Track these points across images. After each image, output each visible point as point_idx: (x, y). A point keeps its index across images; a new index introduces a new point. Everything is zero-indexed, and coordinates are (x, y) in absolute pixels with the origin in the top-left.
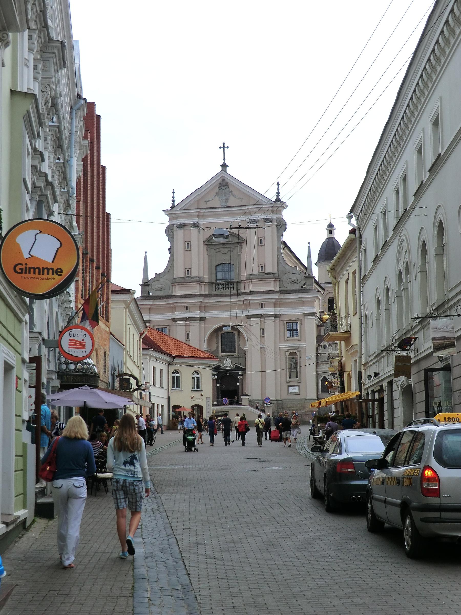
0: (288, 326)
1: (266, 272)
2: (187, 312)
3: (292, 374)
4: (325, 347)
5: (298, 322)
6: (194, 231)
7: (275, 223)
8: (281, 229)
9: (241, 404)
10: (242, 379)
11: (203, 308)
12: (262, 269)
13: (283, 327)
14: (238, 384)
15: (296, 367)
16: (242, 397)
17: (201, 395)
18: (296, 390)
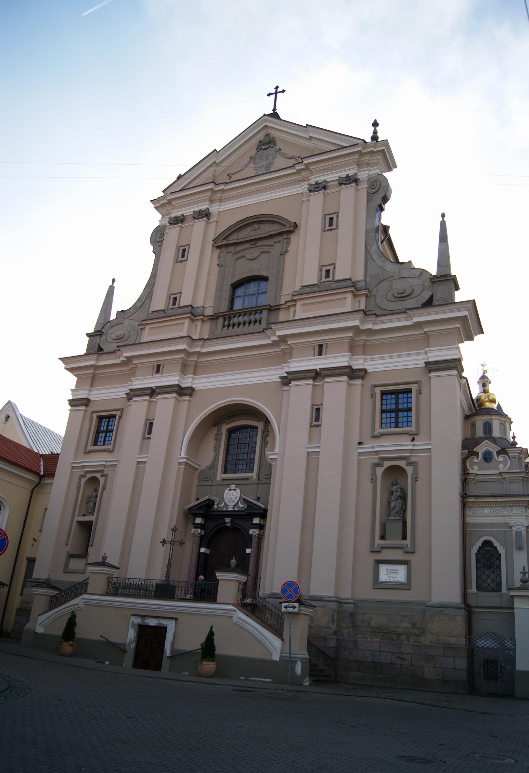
0: (384, 402)
1: (337, 278)
2: (158, 375)
4: (488, 457)
7: (364, 186)
8: (376, 196)
10: (260, 538)
11: (191, 369)
12: (327, 276)
14: (248, 551)
16: (219, 575)
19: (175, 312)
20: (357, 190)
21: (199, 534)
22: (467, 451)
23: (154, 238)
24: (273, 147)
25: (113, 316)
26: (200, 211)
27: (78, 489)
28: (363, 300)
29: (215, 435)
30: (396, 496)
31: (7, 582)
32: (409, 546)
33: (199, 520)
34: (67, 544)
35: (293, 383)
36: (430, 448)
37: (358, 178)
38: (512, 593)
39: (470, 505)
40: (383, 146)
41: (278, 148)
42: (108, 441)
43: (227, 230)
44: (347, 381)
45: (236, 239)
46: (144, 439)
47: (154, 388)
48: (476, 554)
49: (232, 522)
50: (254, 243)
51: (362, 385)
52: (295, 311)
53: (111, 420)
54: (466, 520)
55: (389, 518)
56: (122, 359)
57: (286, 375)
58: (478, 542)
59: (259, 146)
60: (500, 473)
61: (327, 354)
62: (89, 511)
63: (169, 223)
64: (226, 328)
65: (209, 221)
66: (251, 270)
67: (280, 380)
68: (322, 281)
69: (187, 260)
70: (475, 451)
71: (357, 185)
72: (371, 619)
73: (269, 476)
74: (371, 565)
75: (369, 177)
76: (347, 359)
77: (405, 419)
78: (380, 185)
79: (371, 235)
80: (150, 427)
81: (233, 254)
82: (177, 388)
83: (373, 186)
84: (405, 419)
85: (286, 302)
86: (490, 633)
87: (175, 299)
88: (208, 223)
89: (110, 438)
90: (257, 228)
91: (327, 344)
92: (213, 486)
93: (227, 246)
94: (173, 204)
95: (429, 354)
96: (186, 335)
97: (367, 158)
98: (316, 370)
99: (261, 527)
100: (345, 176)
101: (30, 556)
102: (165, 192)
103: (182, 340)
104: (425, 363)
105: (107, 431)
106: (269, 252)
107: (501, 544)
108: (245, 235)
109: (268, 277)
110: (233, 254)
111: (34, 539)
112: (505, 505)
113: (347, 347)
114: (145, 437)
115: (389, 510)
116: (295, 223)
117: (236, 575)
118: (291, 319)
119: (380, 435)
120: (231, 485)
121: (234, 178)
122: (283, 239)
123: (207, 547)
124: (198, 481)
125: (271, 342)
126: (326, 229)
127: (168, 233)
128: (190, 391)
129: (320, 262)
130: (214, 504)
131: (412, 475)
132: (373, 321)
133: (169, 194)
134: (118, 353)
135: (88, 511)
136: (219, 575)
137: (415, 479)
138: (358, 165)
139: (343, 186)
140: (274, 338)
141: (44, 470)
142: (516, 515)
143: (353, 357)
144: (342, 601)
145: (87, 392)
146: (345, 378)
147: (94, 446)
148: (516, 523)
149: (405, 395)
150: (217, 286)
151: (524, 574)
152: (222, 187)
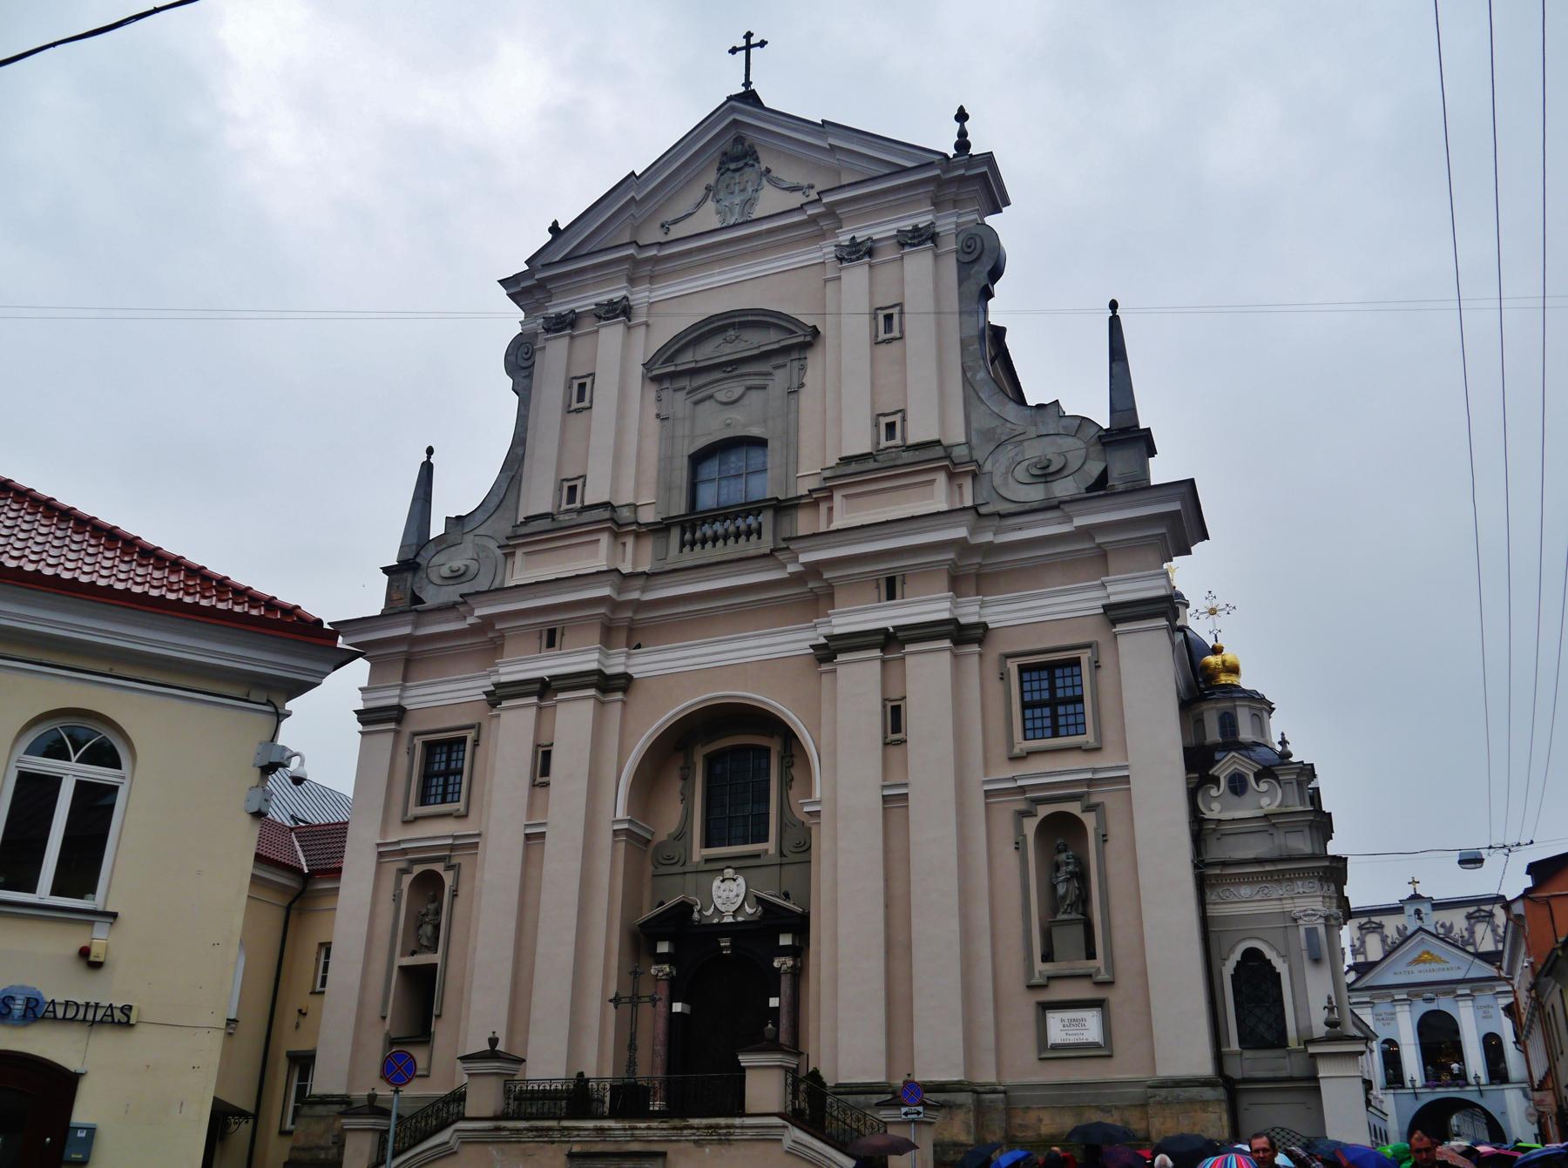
0: (1027, 686)
1: (911, 441)
2: (552, 652)
3: (1057, 933)
4: (1238, 785)
5: (1076, 662)
6: (611, 335)
7: (950, 244)
8: (976, 268)
9: (742, 1114)
11: (623, 637)
13: (995, 687)
14: (774, 1002)
15: (1084, 899)
16: (745, 1059)
17: (84, 953)
18: (1089, 1027)
19: (574, 518)
20: (936, 256)
21: (667, 974)
22: (1197, 775)
23: (513, 358)
24: (753, 166)
25: (437, 528)
26: (611, 302)
27: (397, 898)
28: (967, 484)
29: (682, 768)
30: (1066, 872)
31: (249, 1106)
32: (1103, 970)
33: (663, 948)
34: (384, 1018)
35: (841, 658)
36: (1127, 774)
37: (937, 230)
38: (1312, 1049)
39: (1213, 882)
40: (984, 165)
41: (763, 169)
42: (453, 793)
43: (671, 344)
44: (949, 649)
45: (693, 361)
46: (534, 786)
47: (547, 679)
48: (1232, 975)
49: (732, 947)
50: (729, 369)
51: (981, 655)
52: (831, 509)
53: (455, 748)
54: (1208, 911)
55: (1056, 916)
56: (470, 620)
57: (826, 641)
58: (1233, 952)
59: (722, 163)
60: (1266, 816)
61: (905, 595)
62: (425, 944)
63: (543, 327)
64: (688, 548)
65: (632, 323)
66: (728, 425)
67: (811, 651)
68: (881, 447)
69: (591, 408)
70: (1213, 775)
71: (936, 246)
72: (1040, 1120)
73: (805, 847)
74: (1028, 1013)
75: (959, 230)
76: (947, 605)
77: (1071, 720)
78: (983, 245)
79: (971, 348)
80: (543, 760)
81: (688, 393)
82: (596, 677)
83: (969, 247)
84: (1071, 720)
85: (809, 491)
86: (1278, 1130)
87: (572, 489)
88: (629, 328)
89: (457, 787)
90: (733, 338)
91: (903, 575)
92: (688, 875)
93: (673, 376)
94: (549, 287)
95: (1110, 589)
96: (605, 568)
97: (952, 190)
98: (887, 629)
99: (799, 951)
100: (911, 228)
101: (302, 1046)
102: (532, 264)
103: (603, 578)
104: (1104, 607)
105: (447, 774)
106: (763, 388)
107: (1280, 955)
108: (709, 352)
109: (767, 440)
110: (688, 393)
111: (300, 1011)
112: (1281, 877)
113: (945, 582)
114: (536, 783)
115: (1053, 902)
116: (815, 327)
117: (779, 1056)
118: (823, 529)
119: (1025, 754)
120: (726, 871)
121: (677, 232)
122: (792, 360)
123: (683, 1001)
124: (654, 865)
125: (788, 576)
126: (880, 339)
127: (544, 348)
128: (623, 681)
129: (873, 408)
130: (693, 912)
131: (1096, 829)
132: (994, 528)
133: (540, 267)
134: (462, 609)
135: (422, 945)
136: (745, 1059)
137: (1104, 838)
138: (934, 204)
139: (907, 250)
140: (792, 568)
141: (307, 861)
142: (1303, 895)
143: (959, 600)
144: (979, 1089)
145: (397, 692)
146: (947, 643)
147: (421, 805)
148: (1305, 911)
149: (1068, 671)
150: (660, 460)
151: (1331, 1010)
152: (653, 252)
